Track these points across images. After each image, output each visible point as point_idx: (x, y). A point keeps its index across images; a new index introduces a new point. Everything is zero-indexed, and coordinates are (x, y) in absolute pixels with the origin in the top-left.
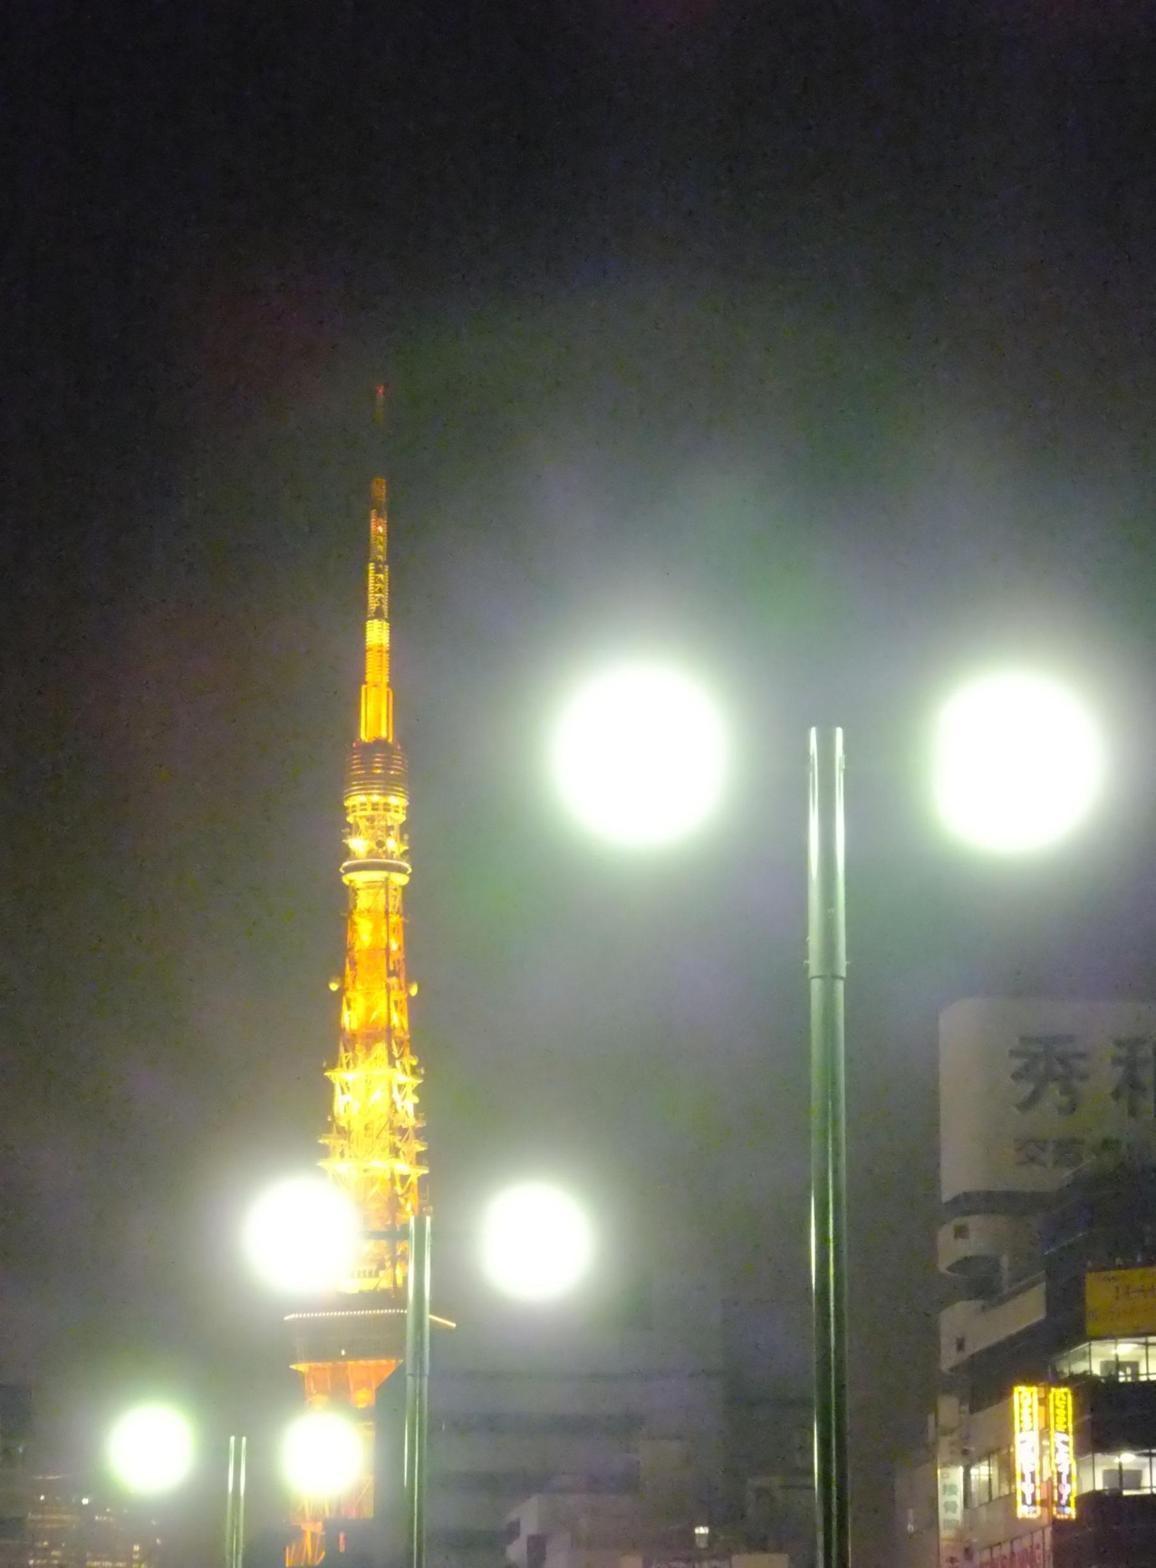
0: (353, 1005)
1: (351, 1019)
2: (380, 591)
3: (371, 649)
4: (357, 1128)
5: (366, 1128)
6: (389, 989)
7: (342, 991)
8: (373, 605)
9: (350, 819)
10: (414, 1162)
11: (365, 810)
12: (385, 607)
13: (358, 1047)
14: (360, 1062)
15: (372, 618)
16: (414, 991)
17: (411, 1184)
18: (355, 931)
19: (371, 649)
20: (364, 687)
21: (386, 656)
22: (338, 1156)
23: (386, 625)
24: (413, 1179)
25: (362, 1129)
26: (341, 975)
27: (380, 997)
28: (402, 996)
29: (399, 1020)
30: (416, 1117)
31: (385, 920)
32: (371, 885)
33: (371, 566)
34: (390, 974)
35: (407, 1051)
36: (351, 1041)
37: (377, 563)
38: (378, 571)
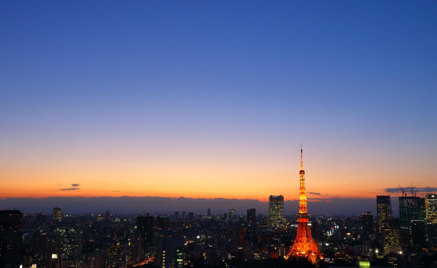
32: (302, 181)
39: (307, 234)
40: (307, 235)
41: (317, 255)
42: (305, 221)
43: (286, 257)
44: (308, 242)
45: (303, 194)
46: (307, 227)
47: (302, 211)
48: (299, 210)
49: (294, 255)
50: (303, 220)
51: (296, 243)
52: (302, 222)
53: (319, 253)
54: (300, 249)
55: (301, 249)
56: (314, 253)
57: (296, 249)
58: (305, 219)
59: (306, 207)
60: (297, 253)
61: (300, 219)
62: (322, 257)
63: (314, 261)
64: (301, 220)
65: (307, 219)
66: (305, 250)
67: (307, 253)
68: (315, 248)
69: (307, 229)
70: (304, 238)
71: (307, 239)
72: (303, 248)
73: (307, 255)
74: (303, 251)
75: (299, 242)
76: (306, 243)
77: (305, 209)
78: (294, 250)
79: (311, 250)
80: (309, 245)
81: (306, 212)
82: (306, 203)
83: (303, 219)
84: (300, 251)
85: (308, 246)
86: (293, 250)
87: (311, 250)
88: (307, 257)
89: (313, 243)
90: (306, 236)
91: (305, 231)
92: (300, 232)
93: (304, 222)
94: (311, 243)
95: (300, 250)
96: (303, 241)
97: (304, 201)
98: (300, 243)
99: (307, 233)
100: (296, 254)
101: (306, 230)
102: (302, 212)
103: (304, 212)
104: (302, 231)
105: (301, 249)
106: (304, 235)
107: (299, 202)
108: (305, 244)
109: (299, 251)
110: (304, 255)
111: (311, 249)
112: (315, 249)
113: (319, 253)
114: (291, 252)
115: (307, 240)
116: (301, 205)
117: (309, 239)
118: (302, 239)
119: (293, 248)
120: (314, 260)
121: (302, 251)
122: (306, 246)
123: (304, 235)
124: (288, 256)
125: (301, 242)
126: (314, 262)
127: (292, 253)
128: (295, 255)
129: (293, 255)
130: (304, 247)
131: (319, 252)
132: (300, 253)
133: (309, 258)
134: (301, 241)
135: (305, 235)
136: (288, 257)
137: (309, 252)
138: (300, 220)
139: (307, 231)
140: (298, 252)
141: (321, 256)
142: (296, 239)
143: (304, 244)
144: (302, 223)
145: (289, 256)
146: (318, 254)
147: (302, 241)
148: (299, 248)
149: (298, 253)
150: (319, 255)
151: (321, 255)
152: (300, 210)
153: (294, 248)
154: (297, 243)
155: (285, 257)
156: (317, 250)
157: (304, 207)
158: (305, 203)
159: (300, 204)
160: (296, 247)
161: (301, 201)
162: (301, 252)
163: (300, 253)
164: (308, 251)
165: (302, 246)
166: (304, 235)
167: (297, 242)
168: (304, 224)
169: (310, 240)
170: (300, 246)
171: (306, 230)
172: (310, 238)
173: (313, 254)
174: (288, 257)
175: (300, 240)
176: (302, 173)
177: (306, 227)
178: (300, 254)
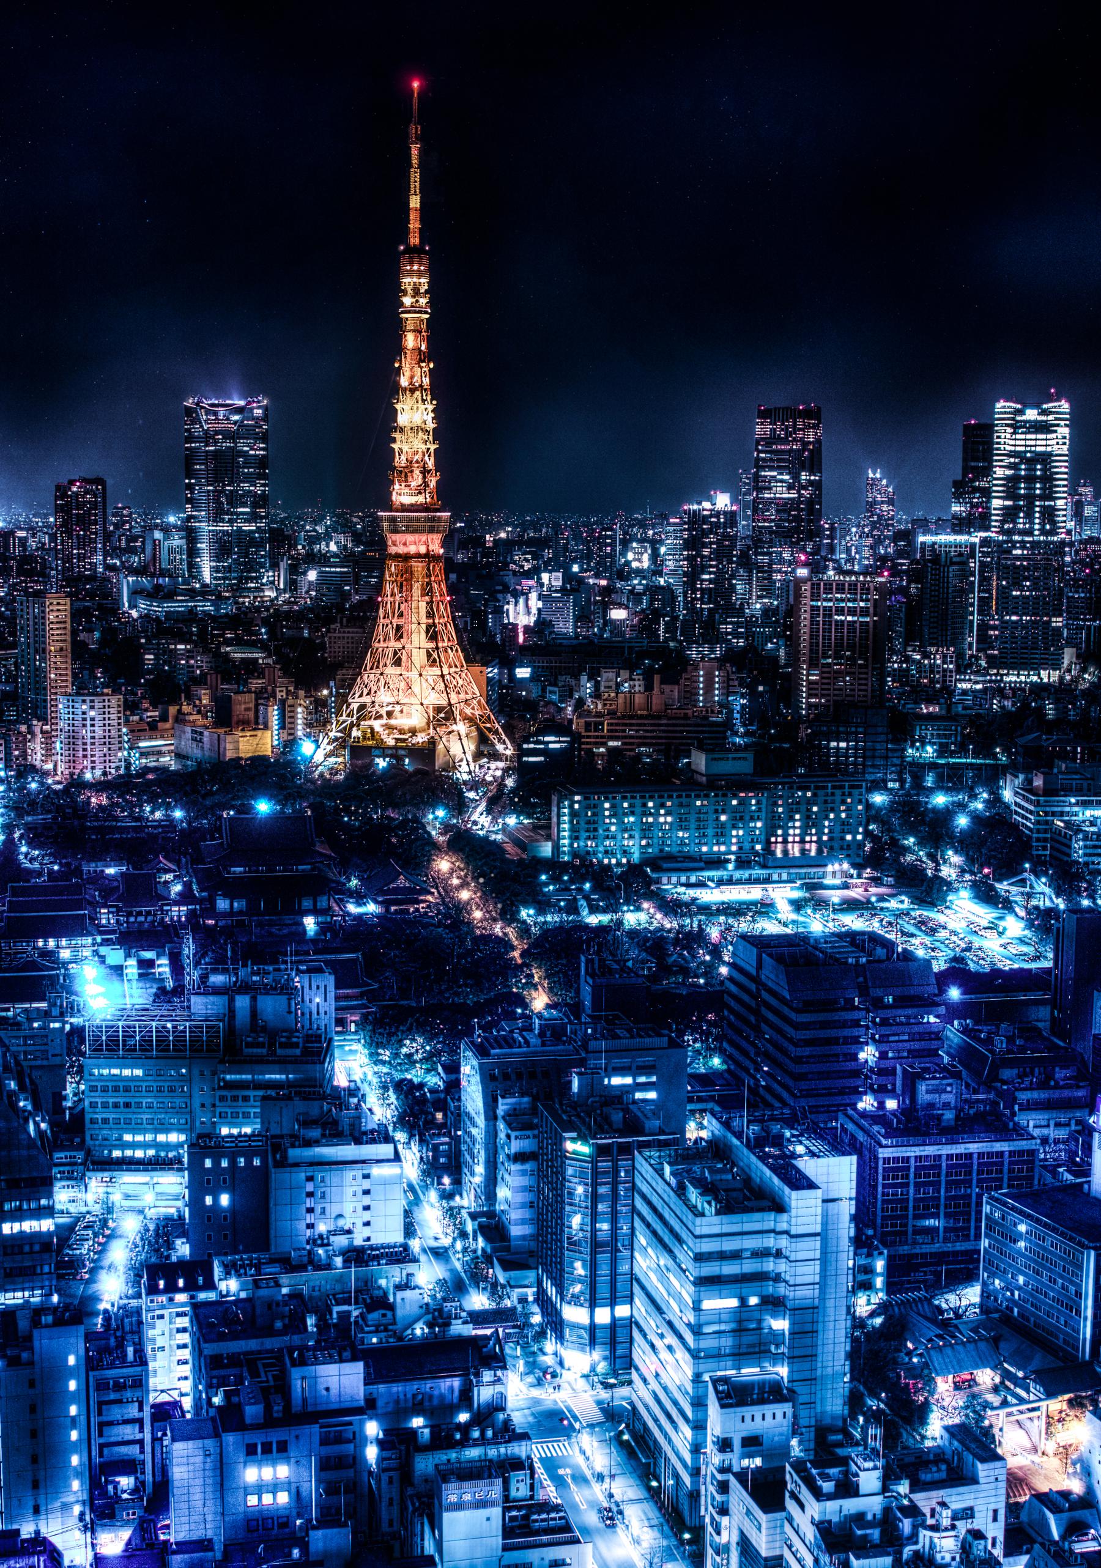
7: (400, 367)
16: (432, 365)
29: (426, 381)
39: (433, 617)
42: (423, 550)
44: (433, 662)
47: (407, 490)
48: (393, 483)
49: (359, 734)
53: (489, 720)
54: (392, 700)
58: (424, 537)
60: (377, 725)
61: (397, 537)
65: (435, 536)
70: (416, 644)
71: (432, 645)
73: (422, 730)
77: (424, 477)
78: (362, 707)
79: (450, 704)
80: (443, 676)
82: (433, 447)
83: (410, 538)
86: (355, 706)
88: (432, 742)
90: (427, 632)
91: (423, 605)
93: (418, 556)
94: (450, 666)
95: (390, 708)
96: (410, 657)
98: (391, 670)
99: (430, 615)
100: (372, 729)
102: (407, 500)
103: (420, 499)
107: (394, 440)
109: (383, 712)
110: (413, 732)
112: (469, 696)
115: (429, 655)
116: (403, 457)
121: (398, 708)
125: (398, 663)
127: (352, 725)
129: (355, 733)
134: (400, 659)
135: (424, 626)
136: (326, 747)
137: (443, 715)
139: (430, 604)
140: (380, 717)
141: (496, 732)
143: (413, 675)
144: (407, 557)
145: (336, 739)
147: (404, 658)
148: (384, 697)
150: (489, 730)
152: (397, 486)
158: (424, 447)
164: (438, 709)
166: (414, 626)
168: (418, 567)
171: (427, 598)
174: (331, 747)
175: (395, 653)
176: (415, 268)
178: (390, 728)
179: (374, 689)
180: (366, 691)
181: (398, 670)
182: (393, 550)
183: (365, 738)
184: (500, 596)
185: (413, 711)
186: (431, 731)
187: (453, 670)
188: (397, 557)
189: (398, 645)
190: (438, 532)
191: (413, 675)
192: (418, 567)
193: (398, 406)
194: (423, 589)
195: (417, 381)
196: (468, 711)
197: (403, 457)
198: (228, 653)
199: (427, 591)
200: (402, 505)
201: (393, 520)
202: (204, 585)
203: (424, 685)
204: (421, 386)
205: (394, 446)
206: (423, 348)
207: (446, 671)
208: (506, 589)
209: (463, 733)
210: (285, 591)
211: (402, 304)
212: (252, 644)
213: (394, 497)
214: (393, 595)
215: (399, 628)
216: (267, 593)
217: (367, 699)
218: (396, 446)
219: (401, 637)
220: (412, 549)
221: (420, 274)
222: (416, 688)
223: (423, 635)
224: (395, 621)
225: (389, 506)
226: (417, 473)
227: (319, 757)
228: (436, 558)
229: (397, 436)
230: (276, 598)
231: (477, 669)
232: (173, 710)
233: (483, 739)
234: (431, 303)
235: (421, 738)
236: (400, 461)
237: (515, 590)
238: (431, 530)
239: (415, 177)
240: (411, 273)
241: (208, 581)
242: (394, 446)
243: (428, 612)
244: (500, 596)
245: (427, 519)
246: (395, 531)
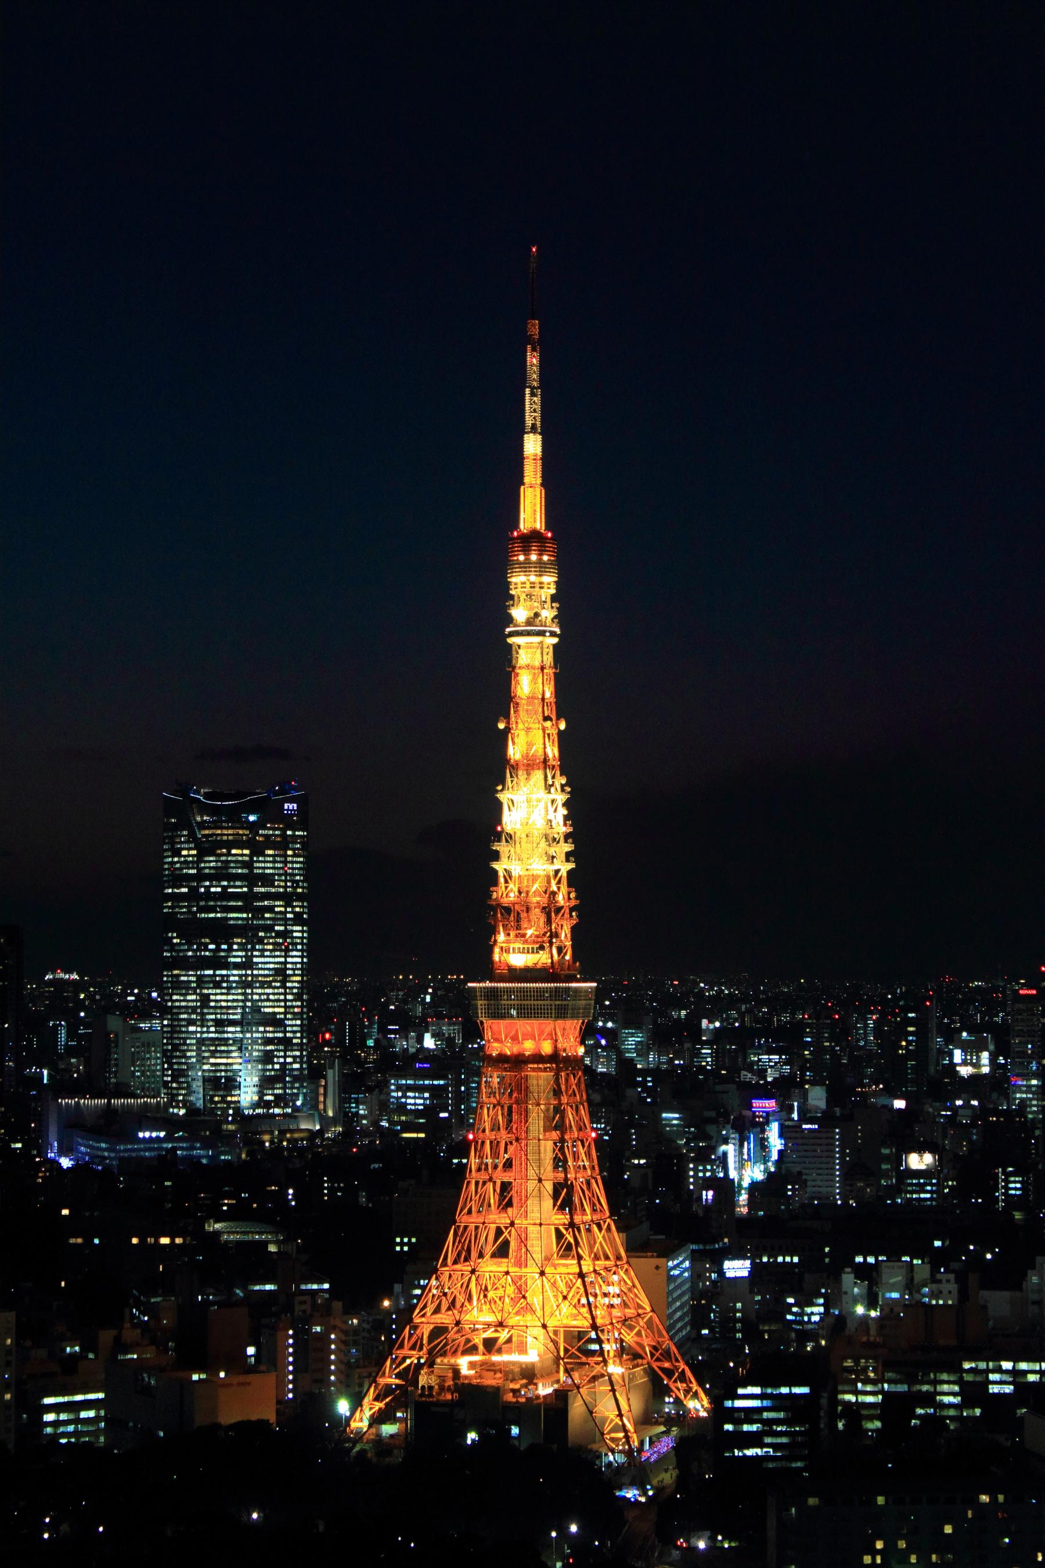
0: (516, 740)
1: (515, 752)
2: (535, 411)
3: (528, 458)
4: (520, 834)
5: (527, 836)
6: (544, 729)
7: (508, 730)
8: (529, 422)
9: (512, 592)
10: (564, 860)
11: (525, 587)
12: (538, 424)
13: (520, 773)
14: (522, 784)
15: (528, 433)
16: (562, 726)
17: (561, 876)
18: (517, 683)
19: (528, 458)
20: (522, 487)
21: (539, 463)
22: (507, 859)
23: (539, 437)
24: (563, 873)
25: (524, 836)
26: (507, 717)
27: (538, 736)
28: (555, 732)
29: (553, 751)
30: (565, 825)
31: (541, 675)
32: (529, 646)
33: (528, 391)
34: (546, 719)
35: (558, 772)
36: (515, 767)
37: (532, 388)
38: (533, 394)
39: (566, 1172)
40: (566, 1179)
41: (652, 1375)
42: (547, 1048)
43: (357, 1404)
44: (567, 1250)
45: (538, 775)
46: (564, 1099)
48: (494, 931)
49: (433, 1381)
50: (526, 1037)
51: (455, 1262)
52: (516, 1050)
53: (667, 1355)
54: (491, 1318)
55: (501, 1324)
56: (628, 1354)
57: (458, 1323)
58: (549, 1025)
59: (559, 910)
60: (464, 1364)
61: (502, 1025)
62: (695, 1387)
63: (621, 1435)
64: (515, 1039)
66: (544, 1326)
67: (558, 1358)
68: (640, 1307)
69: (561, 1127)
70: (534, 1216)
71: (563, 1219)
72: (529, 1309)
73: (549, 1374)
74: (522, 1349)
75: (481, 1256)
76: (548, 1259)
77: (549, 921)
78: (439, 1331)
79: (594, 1327)
80: (581, 1275)
81: (560, 950)
82: (565, 868)
84: (490, 1345)
85: (570, 1288)
86: (426, 1331)
87: (594, 1327)
88: (561, 1396)
89: (619, 1258)
90: (556, 1196)
91: (548, 1148)
92: (495, 1154)
93: (538, 1058)
94: (597, 1258)
95: (489, 1334)
96: (523, 1241)
97: (543, 844)
98: (489, 1267)
99: (560, 1162)
100: (456, 1372)
101: (555, 1135)
102: (519, 960)
103: (543, 958)
104: (517, 1140)
105: (501, 1324)
106: (540, 1180)
107: (496, 856)
108: (542, 1273)
109: (478, 1340)
110: (529, 1374)
111: (593, 1318)
112: (630, 1312)
113: (667, 1355)
114: (405, 1352)
115: (559, 1235)
116: (513, 887)
117: (577, 1219)
118: (512, 1224)
119: (429, 1310)
120: (624, 1428)
121: (503, 1335)
122: (554, 1284)
123: (532, 1185)
124: (377, 1399)
125: (502, 1251)
126: (627, 1437)
128: (442, 1378)
129: (423, 1380)
130: (538, 1307)
131: (667, 1343)
132: (496, 1358)
133: (576, 1408)
134: (506, 1243)
135: (549, 1186)
136: (370, 1407)
138: (497, 1040)
140: (472, 1350)
141: (682, 1377)
142: (455, 1222)
143: (531, 1271)
144: (518, 1062)
145: (388, 1390)
146: (655, 1365)
149: (472, 1365)
150: (669, 1373)
151: (689, 1373)
152: (501, 937)
153: (437, 1311)
154: (467, 1268)
155: (343, 1407)
156: (650, 1323)
157: (544, 900)
158: (551, 868)
159: (508, 877)
160: (452, 1305)
161: (510, 837)
162: (499, 1351)
163: (496, 1358)
165: (511, 1290)
166: (532, 1185)
167: (464, 1255)
168: (540, 1079)
169: (589, 1230)
170: (491, 1294)
171: (555, 1135)
172: (594, 1211)
173: (615, 1369)
174: (378, 1405)
175: (499, 1232)
176: (534, 557)
177: (558, 1109)
179: (461, 1299)
180: (445, 1305)
181: (503, 1265)
182: (495, 1049)
183: (442, 1388)
184: (711, 1129)
185: (530, 1340)
186: (562, 1377)
187: (601, 1263)
188: (502, 1060)
189: (503, 1220)
190: (574, 1016)
191: (531, 1271)
192: (540, 1079)
193: (504, 797)
194: (548, 1120)
195: (537, 749)
196: (629, 1338)
197: (513, 887)
198: (217, 1234)
199: (557, 1123)
200: (512, 969)
201: (492, 995)
202: (192, 1111)
203: (550, 1293)
204: (545, 761)
205: (496, 866)
206: (548, 695)
207: (587, 1266)
208: (722, 1117)
209: (616, 1378)
210: (334, 1121)
211: (509, 620)
212: (262, 1218)
213: (496, 957)
214: (495, 1127)
215: (506, 1187)
216: (303, 1126)
217: (444, 1318)
218: (499, 867)
219: (510, 1204)
220: (529, 1047)
221: (541, 568)
222: (535, 1298)
223: (548, 1203)
224: (501, 1176)
225: (486, 968)
226: (537, 914)
227: (361, 1423)
228: (573, 1062)
229: (501, 847)
230: (321, 1132)
231: (648, 1263)
232: (106, 1337)
233: (657, 1389)
234: (560, 618)
235: (544, 1390)
236: (506, 893)
237: (740, 1118)
238: (561, 1013)
239: (532, 408)
240: (526, 567)
241: (200, 1104)
242: (496, 866)
243: (556, 1160)
244: (711, 1129)
245: (556, 993)
246: (498, 1014)
